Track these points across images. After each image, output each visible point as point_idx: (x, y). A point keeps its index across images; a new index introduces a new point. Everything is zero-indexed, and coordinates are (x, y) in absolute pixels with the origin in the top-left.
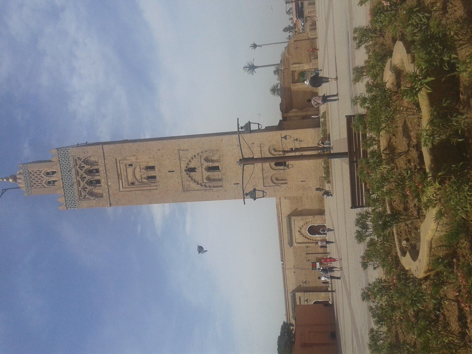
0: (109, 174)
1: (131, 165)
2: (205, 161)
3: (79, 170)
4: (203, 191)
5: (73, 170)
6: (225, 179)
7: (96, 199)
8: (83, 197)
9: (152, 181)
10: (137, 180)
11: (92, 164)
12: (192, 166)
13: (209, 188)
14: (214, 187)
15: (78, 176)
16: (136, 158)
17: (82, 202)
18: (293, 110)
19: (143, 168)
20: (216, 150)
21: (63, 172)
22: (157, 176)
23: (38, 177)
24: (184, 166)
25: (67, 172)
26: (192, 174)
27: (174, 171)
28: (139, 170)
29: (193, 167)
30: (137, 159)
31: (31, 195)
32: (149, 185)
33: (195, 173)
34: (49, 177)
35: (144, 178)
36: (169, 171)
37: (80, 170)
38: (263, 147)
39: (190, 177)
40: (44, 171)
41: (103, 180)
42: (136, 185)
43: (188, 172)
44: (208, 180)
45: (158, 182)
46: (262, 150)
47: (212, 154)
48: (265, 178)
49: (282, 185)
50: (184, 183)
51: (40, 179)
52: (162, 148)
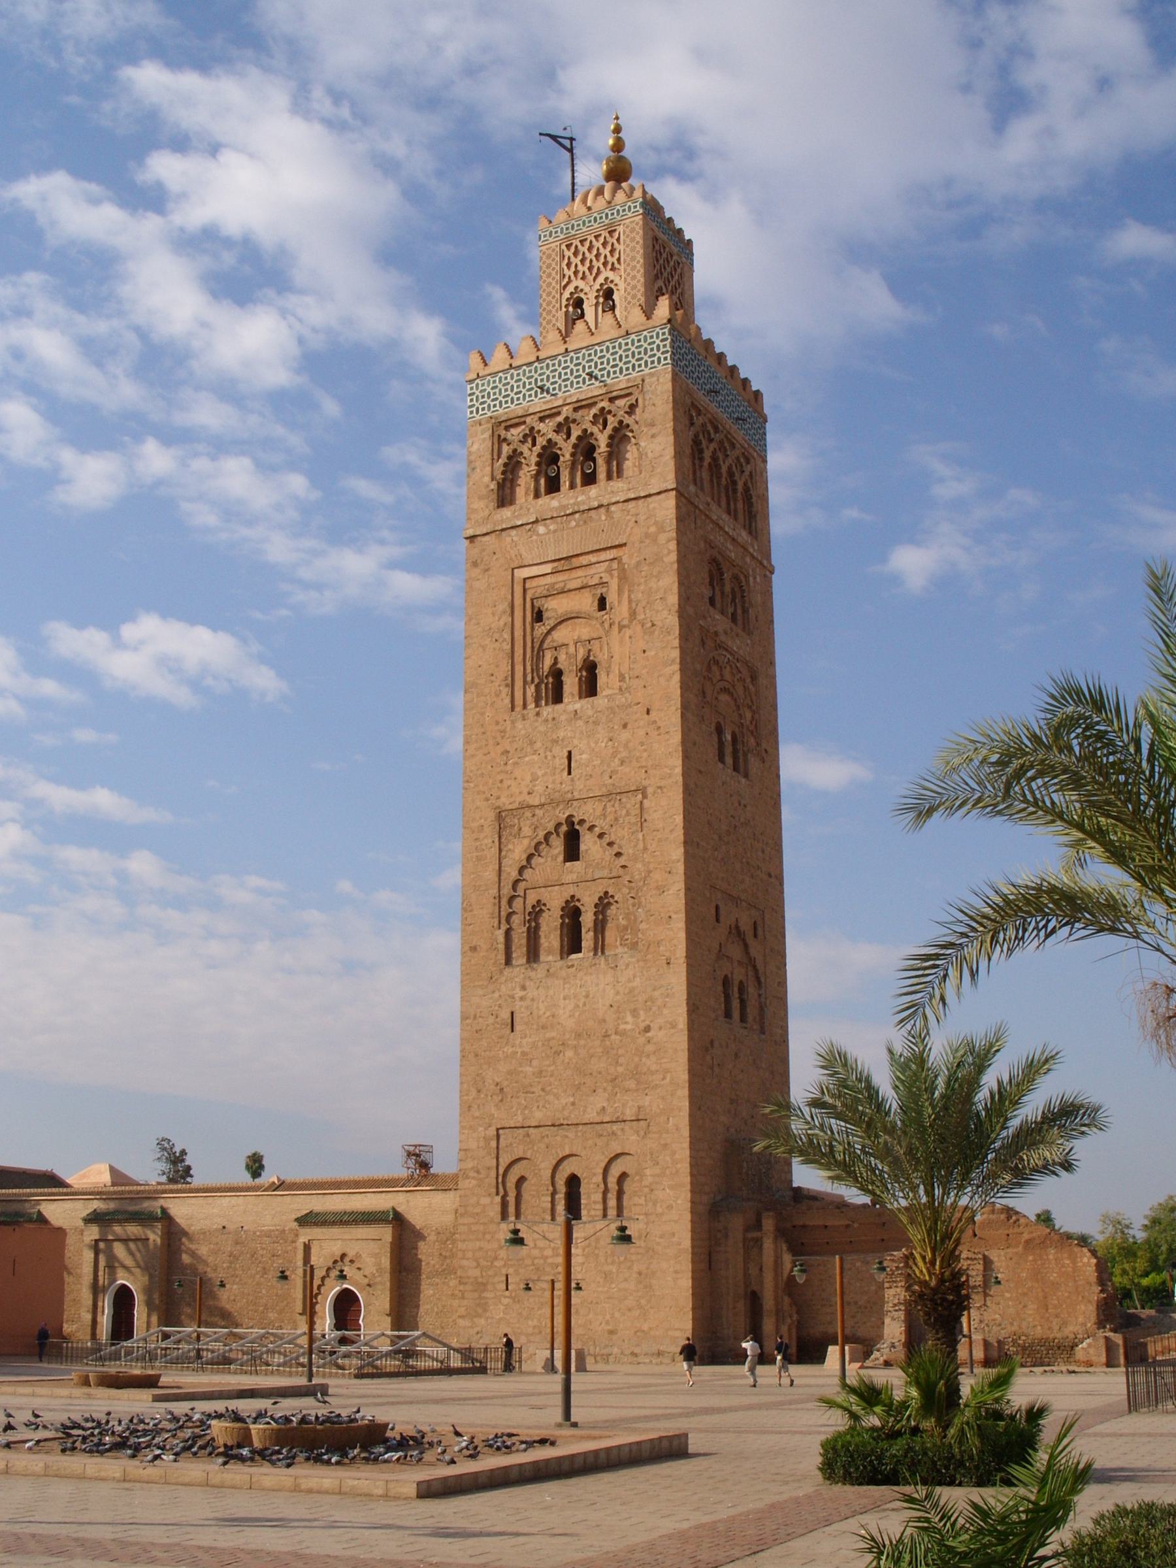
0: (573, 523)
1: (602, 604)
2: (600, 898)
3: (594, 411)
4: (495, 892)
5: (595, 389)
6: (532, 974)
7: (493, 486)
8: (503, 433)
9: (543, 686)
10: (549, 632)
11: (616, 453)
12: (588, 843)
13: (504, 914)
14: (508, 933)
15: (576, 410)
16: (625, 622)
17: (487, 434)
18: (787, 1258)
19: (590, 651)
20: (637, 942)
21: (590, 355)
22: (559, 707)
23: (598, 260)
24: (587, 812)
25: (590, 367)
26: (558, 845)
27: (569, 773)
28: (585, 637)
29: (583, 847)
30: (621, 628)
31: (540, 243)
32: (529, 678)
33: (561, 858)
34: (594, 301)
35: (556, 658)
36: (570, 753)
37: (595, 416)
38: (637, 1132)
39: (547, 836)
40: (617, 280)
41: (555, 503)
42: (533, 629)
43: (564, 828)
44: (533, 907)
45: (538, 714)
46: (627, 1126)
47: (624, 922)
48: (528, 1135)
49: (498, 1199)
50: (528, 814)
51: (590, 269)
52: (655, 722)
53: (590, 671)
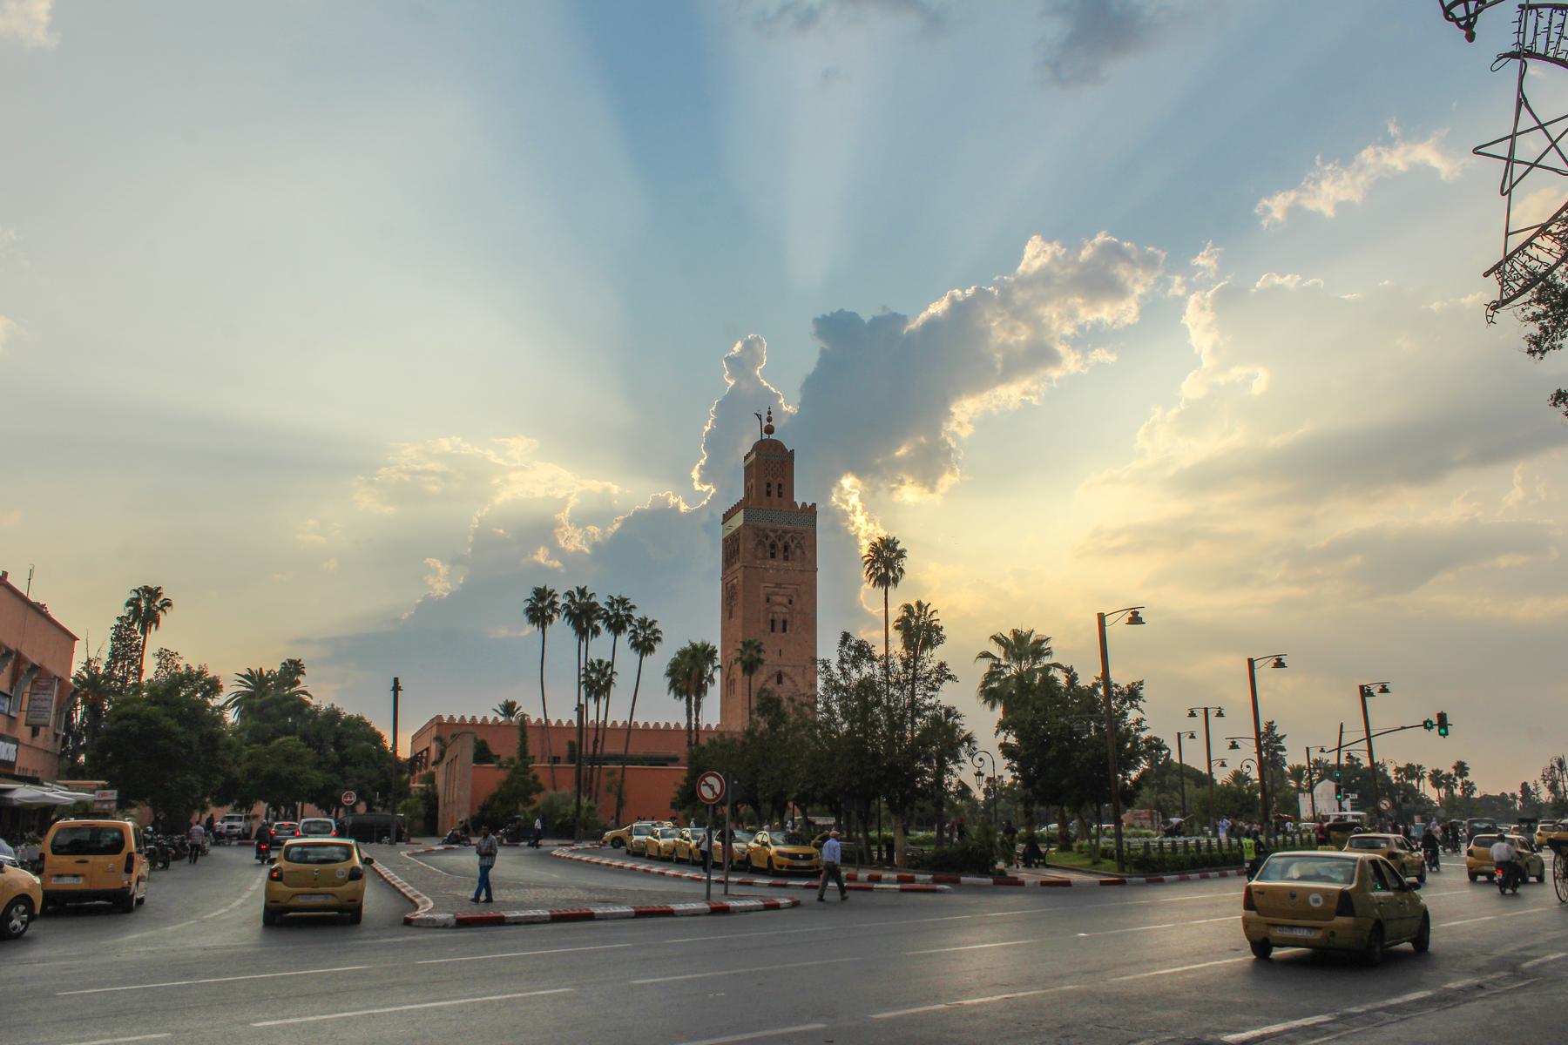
5: (790, 527)
12: (785, 679)
24: (787, 670)
53: (785, 622)
